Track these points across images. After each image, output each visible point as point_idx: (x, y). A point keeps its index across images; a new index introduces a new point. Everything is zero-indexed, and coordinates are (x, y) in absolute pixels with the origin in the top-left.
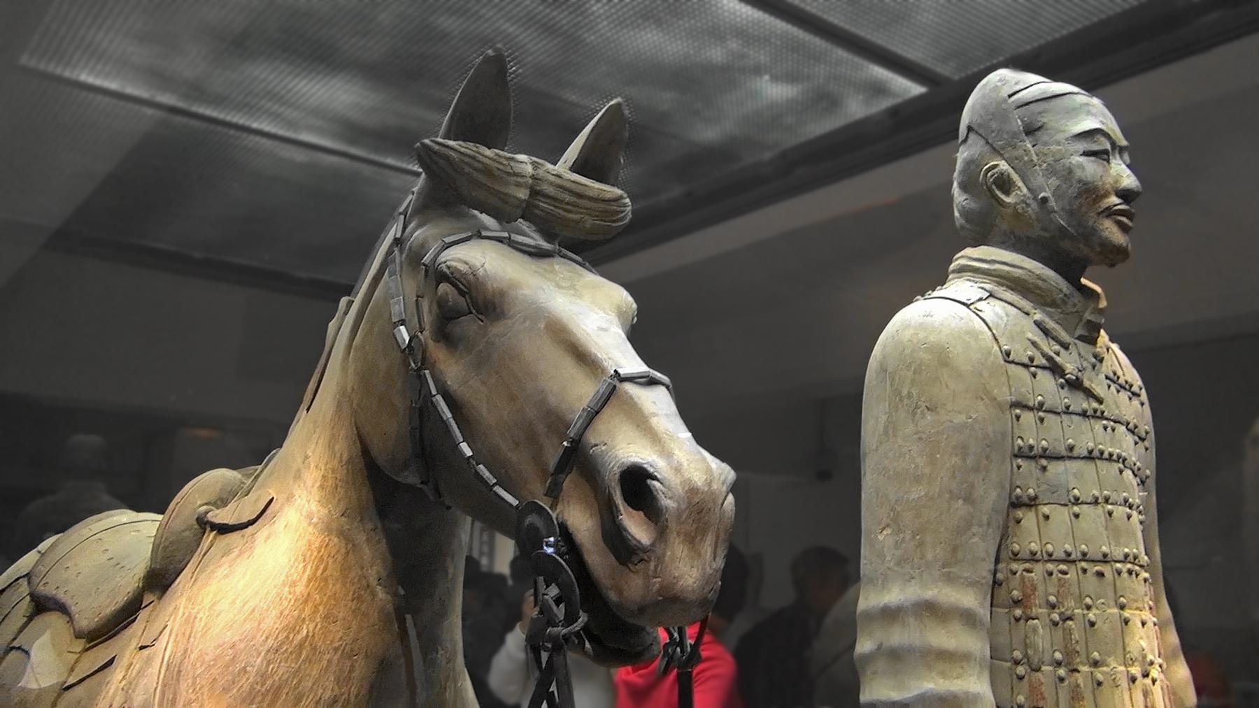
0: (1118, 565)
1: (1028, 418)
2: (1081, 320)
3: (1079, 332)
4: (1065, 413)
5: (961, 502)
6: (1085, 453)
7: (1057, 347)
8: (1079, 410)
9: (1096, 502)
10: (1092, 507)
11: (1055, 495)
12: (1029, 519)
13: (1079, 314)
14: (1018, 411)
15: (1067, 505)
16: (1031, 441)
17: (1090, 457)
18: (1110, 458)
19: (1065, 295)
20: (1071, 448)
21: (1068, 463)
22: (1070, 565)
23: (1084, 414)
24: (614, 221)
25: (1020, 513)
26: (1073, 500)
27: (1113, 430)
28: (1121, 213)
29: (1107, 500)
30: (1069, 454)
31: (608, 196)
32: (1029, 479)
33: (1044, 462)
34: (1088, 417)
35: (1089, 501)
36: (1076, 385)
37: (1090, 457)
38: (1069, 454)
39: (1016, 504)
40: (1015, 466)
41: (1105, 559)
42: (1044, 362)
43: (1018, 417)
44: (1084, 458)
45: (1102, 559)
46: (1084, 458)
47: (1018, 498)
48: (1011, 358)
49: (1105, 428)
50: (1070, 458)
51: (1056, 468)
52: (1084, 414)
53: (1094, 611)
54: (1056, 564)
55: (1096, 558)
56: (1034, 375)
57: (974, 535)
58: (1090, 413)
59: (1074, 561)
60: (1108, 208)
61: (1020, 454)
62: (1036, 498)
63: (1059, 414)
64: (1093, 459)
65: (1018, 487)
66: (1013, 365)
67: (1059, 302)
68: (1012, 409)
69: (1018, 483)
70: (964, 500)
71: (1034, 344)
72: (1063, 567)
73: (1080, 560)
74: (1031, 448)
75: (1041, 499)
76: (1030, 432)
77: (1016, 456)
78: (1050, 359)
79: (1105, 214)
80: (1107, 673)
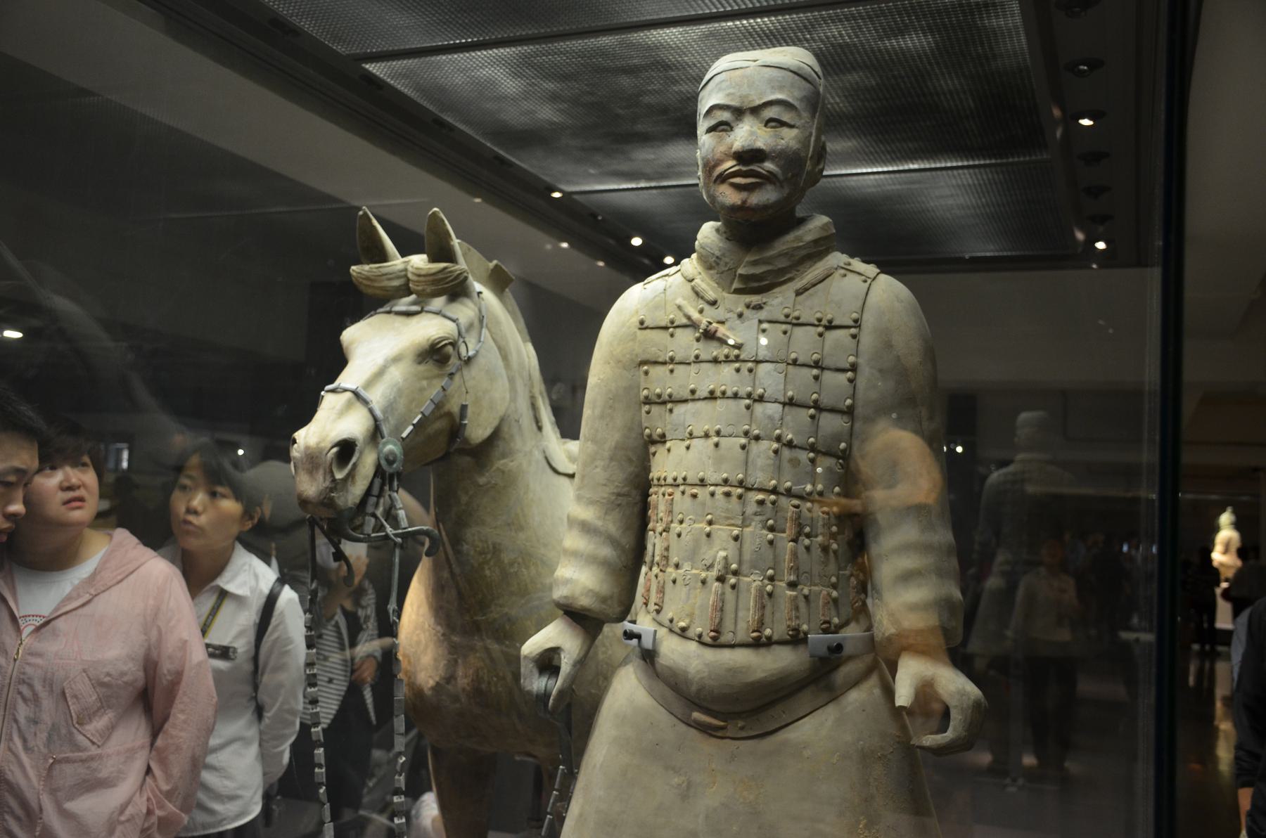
0: (712, 488)
1: (657, 371)
2: (735, 275)
3: (736, 285)
4: (694, 362)
5: (590, 442)
6: (706, 394)
7: (702, 305)
8: (709, 357)
9: (707, 436)
10: (702, 441)
11: (677, 432)
12: (660, 451)
13: (732, 270)
14: (646, 368)
15: (684, 440)
16: (658, 391)
17: (712, 396)
18: (736, 396)
19: (717, 257)
20: (693, 392)
21: (690, 405)
22: (675, 488)
23: (715, 361)
24: (447, 283)
25: (652, 449)
26: (688, 436)
27: (750, 371)
28: (735, 174)
29: (718, 433)
30: (693, 396)
31: (433, 271)
32: (657, 421)
33: (669, 406)
34: (720, 362)
35: (699, 435)
36: (709, 335)
37: (712, 396)
38: (693, 396)
39: (654, 442)
40: (643, 411)
41: (702, 483)
42: (684, 321)
43: (646, 373)
44: (705, 398)
45: (699, 483)
46: (705, 398)
47: (650, 436)
48: (645, 325)
49: (738, 370)
50: (693, 400)
51: (680, 409)
52: (715, 361)
53: (684, 525)
54: (668, 487)
55: (733, 484)
56: (672, 335)
57: (596, 467)
58: (722, 358)
59: (678, 486)
60: (721, 175)
61: (647, 401)
62: (663, 436)
63: (689, 364)
64: (715, 398)
65: (646, 428)
66: (648, 331)
67: (714, 264)
68: (641, 367)
69: (645, 425)
70: (592, 441)
71: (679, 307)
72: (670, 490)
73: (682, 484)
74: (659, 396)
75: (668, 436)
76: (661, 382)
77: (645, 403)
78: (689, 318)
79: (718, 182)
80: (680, 574)
